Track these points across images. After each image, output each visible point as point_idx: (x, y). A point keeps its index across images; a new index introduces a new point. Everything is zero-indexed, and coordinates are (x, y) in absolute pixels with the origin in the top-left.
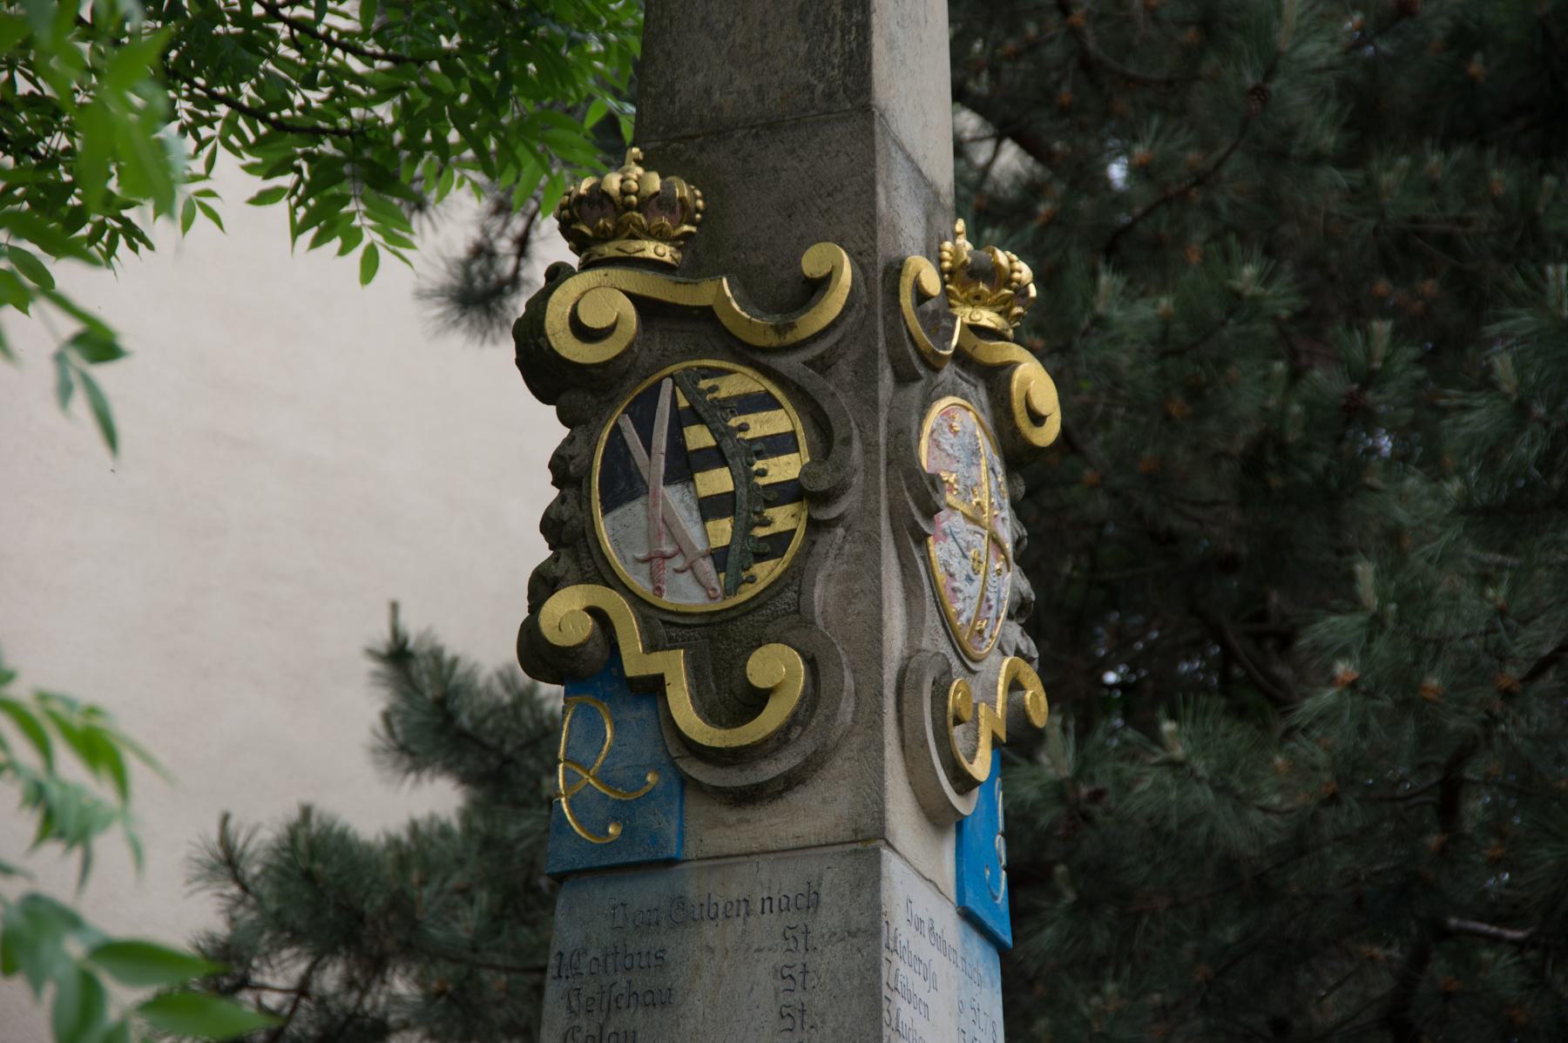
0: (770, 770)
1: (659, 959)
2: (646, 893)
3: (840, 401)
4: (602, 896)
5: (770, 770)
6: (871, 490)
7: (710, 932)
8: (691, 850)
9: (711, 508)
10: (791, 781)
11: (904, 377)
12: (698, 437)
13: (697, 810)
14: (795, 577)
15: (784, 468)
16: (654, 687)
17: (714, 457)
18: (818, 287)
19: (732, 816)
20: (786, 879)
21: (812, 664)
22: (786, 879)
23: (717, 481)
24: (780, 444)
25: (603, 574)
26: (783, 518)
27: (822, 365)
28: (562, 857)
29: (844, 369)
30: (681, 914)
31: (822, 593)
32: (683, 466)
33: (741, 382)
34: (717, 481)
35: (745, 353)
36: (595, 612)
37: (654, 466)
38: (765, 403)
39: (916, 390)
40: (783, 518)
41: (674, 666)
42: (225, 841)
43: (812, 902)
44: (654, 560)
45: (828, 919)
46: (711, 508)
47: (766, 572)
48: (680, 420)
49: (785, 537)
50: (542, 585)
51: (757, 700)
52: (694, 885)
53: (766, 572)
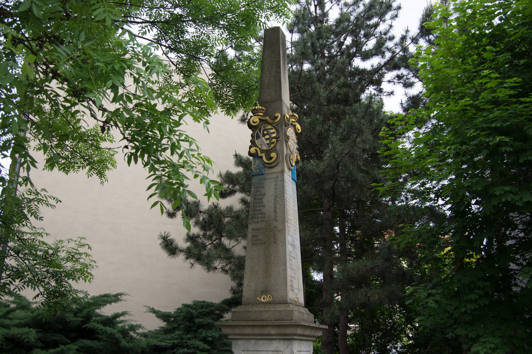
0: (273, 165)
1: (263, 183)
2: (261, 177)
3: (279, 129)
4: (257, 177)
5: (273, 165)
6: (282, 137)
7: (268, 181)
9: (267, 139)
10: (275, 166)
11: (286, 126)
12: (265, 132)
13: (266, 169)
14: (275, 146)
15: (274, 135)
16: (261, 157)
17: (267, 134)
18: (277, 117)
19: (269, 169)
20: (275, 175)
21: (277, 154)
22: (275, 175)
23: (267, 137)
25: (256, 146)
26: (274, 140)
27: (277, 125)
28: (253, 174)
29: (280, 125)
30: (265, 179)
31: (278, 147)
32: (264, 135)
33: (269, 127)
34: (267, 137)
35: (270, 124)
36: (256, 150)
37: (261, 135)
38: (272, 129)
39: (287, 127)
40: (274, 140)
41: (263, 155)
42: (220, 173)
43: (277, 178)
44: (261, 145)
45: (279, 179)
46: (267, 139)
47: (272, 145)
48: (263, 131)
49: (274, 142)
50: (250, 147)
51: (272, 158)
52: (266, 176)
53: (272, 145)
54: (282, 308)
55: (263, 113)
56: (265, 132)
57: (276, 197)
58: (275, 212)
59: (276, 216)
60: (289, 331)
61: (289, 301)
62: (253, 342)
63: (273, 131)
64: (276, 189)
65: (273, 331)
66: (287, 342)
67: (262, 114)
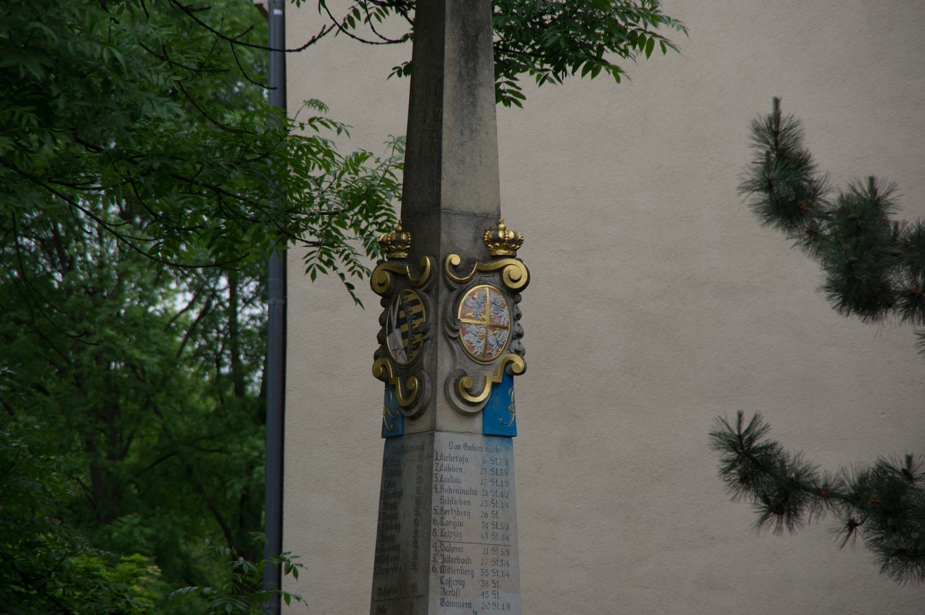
0: (414, 411)
5: (414, 411)
8: (405, 432)
11: (451, 289)
21: (420, 381)
23: (405, 327)
24: (419, 315)
26: (418, 338)
31: (426, 359)
32: (400, 322)
35: (415, 286)
39: (454, 294)
44: (395, 350)
47: (415, 353)
49: (418, 344)
53: (415, 353)
55: (407, 250)
56: (402, 315)
57: (418, 502)
58: (415, 542)
59: (416, 557)
64: (419, 478)
67: (404, 255)
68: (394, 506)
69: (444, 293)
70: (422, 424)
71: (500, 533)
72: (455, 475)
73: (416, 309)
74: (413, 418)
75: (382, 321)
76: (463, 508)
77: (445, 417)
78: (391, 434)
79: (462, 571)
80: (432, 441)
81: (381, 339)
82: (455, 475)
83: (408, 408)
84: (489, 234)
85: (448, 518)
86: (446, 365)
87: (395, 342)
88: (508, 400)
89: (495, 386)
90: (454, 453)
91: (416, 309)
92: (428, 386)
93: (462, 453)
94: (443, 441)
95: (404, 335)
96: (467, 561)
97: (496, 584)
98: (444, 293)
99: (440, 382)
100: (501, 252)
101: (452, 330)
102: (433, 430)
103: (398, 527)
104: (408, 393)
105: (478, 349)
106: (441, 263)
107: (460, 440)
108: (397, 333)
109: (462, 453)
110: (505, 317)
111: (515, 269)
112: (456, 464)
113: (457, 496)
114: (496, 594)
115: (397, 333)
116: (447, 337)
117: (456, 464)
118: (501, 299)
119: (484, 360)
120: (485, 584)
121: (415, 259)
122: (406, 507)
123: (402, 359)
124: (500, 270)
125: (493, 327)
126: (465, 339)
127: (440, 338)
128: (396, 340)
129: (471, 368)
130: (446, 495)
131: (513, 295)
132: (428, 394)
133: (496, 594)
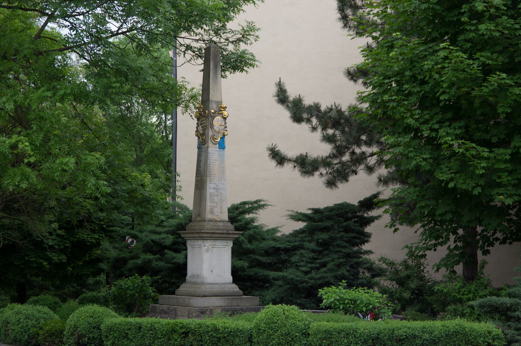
11: (212, 117)
14: (205, 131)
23: (202, 125)
24: (205, 123)
26: (205, 128)
31: (206, 132)
32: (201, 124)
35: (204, 117)
40: (205, 128)
54: (202, 223)
57: (205, 162)
59: (204, 174)
60: (202, 235)
61: (206, 219)
62: (193, 241)
63: (205, 121)
64: (205, 157)
65: (196, 235)
66: (203, 241)
67: (202, 110)
68: (200, 163)
69: (210, 118)
70: (206, 146)
71: (222, 169)
72: (213, 157)
73: (204, 122)
74: (204, 145)
75: (197, 124)
76: (214, 163)
77: (210, 144)
78: (199, 148)
79: (214, 177)
80: (208, 150)
81: (197, 128)
82: (213, 157)
83: (203, 142)
84: (220, 106)
85: (211, 165)
86: (210, 134)
87: (200, 128)
88: (224, 141)
89: (221, 138)
90: (212, 152)
91: (204, 122)
92: (207, 138)
93: (214, 152)
94: (210, 149)
95: (202, 127)
96: (215, 174)
97: (221, 179)
98: (210, 118)
99: (209, 137)
100: (222, 110)
101: (212, 126)
102: (208, 147)
103: (200, 167)
104: (203, 139)
105: (217, 130)
106: (209, 112)
107: (213, 149)
108: (200, 127)
109: (214, 152)
110: (223, 123)
111: (225, 113)
112: (213, 154)
113: (213, 161)
114: (221, 181)
115: (200, 127)
116: (211, 128)
117: (213, 154)
118: (222, 120)
119: (219, 132)
120: (219, 179)
121: (204, 111)
122: (202, 163)
123: (201, 132)
124: (222, 113)
125: (221, 125)
126: (215, 128)
127: (209, 128)
128: (200, 128)
129: (216, 134)
130: (211, 161)
131: (225, 119)
132: (207, 140)
133: (221, 181)
